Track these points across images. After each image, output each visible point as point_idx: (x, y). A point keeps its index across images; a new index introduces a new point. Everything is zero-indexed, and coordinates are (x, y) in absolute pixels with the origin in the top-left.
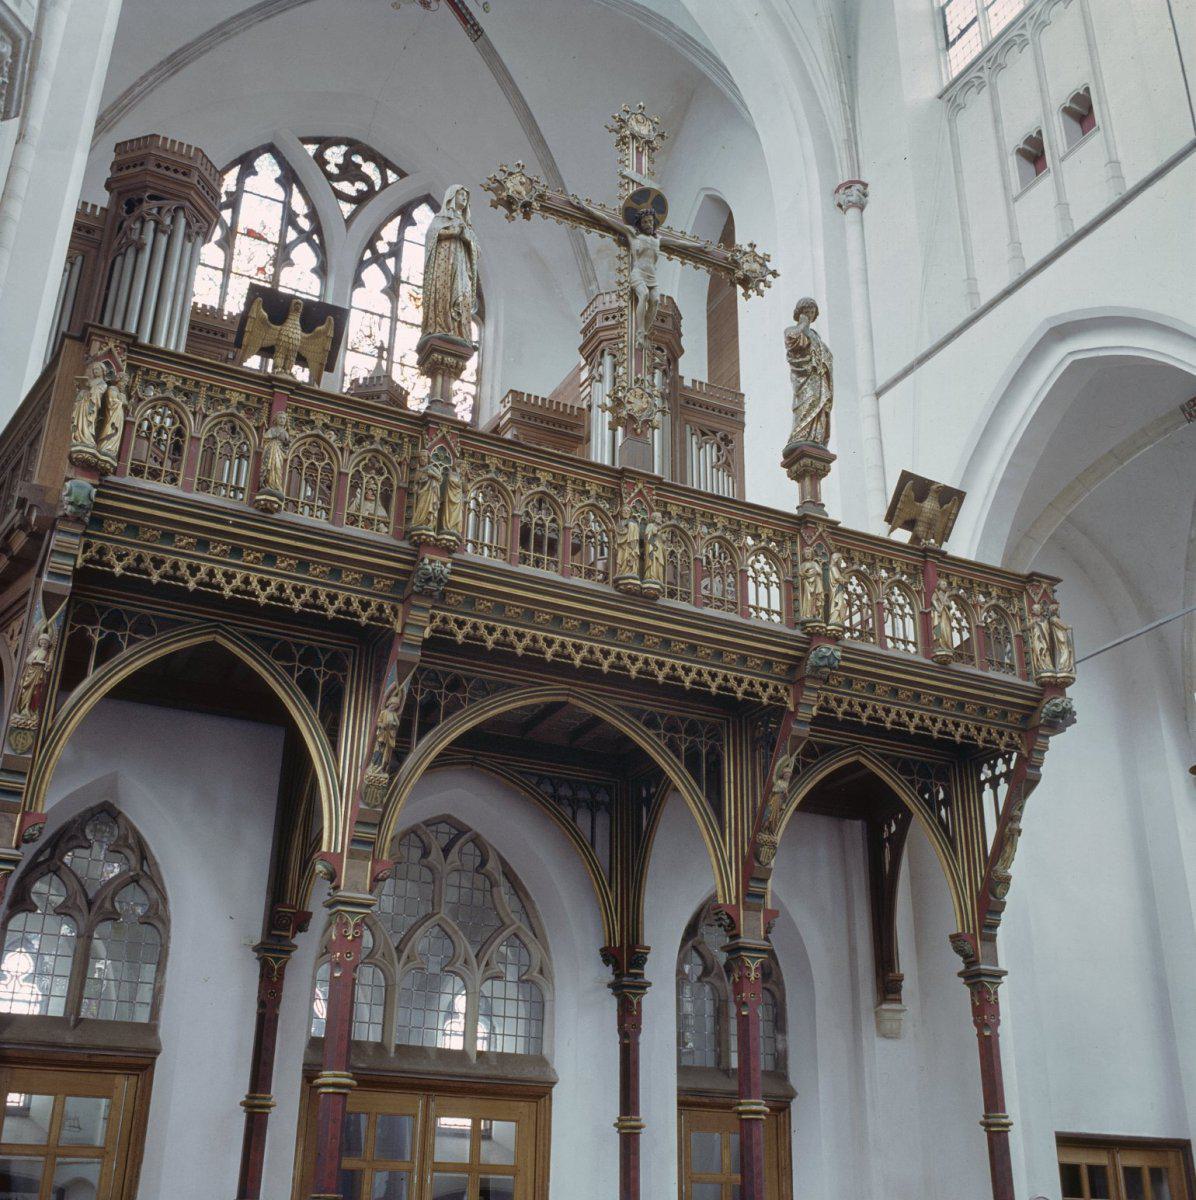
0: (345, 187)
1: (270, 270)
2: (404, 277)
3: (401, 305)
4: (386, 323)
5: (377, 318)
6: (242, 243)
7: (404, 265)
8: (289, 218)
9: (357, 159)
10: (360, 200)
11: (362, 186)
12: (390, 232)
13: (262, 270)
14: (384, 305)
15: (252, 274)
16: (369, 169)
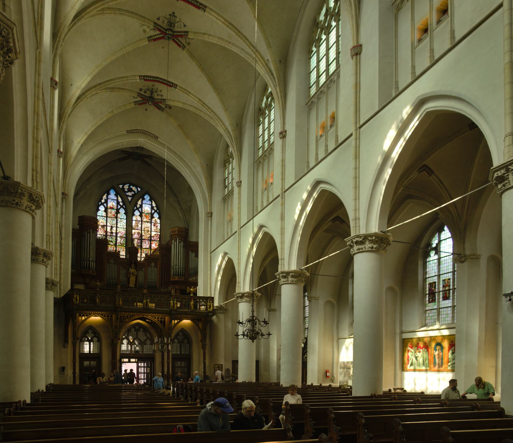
0: (130, 194)
1: (116, 215)
2: (143, 211)
3: (143, 218)
4: (140, 222)
5: (138, 222)
6: (109, 210)
7: (143, 209)
8: (118, 203)
9: (131, 187)
10: (133, 196)
11: (133, 193)
12: (139, 202)
13: (114, 215)
14: (139, 218)
15: (112, 216)
16: (134, 188)
